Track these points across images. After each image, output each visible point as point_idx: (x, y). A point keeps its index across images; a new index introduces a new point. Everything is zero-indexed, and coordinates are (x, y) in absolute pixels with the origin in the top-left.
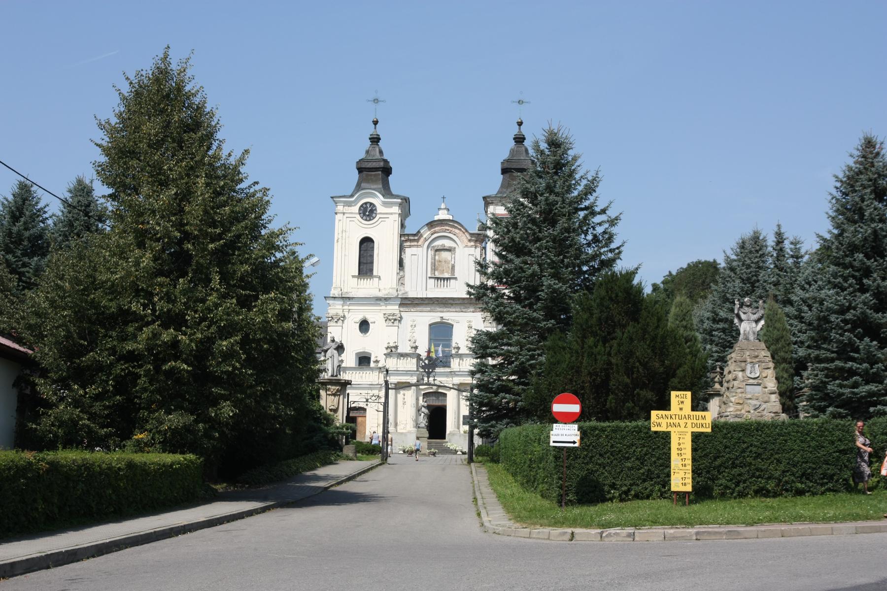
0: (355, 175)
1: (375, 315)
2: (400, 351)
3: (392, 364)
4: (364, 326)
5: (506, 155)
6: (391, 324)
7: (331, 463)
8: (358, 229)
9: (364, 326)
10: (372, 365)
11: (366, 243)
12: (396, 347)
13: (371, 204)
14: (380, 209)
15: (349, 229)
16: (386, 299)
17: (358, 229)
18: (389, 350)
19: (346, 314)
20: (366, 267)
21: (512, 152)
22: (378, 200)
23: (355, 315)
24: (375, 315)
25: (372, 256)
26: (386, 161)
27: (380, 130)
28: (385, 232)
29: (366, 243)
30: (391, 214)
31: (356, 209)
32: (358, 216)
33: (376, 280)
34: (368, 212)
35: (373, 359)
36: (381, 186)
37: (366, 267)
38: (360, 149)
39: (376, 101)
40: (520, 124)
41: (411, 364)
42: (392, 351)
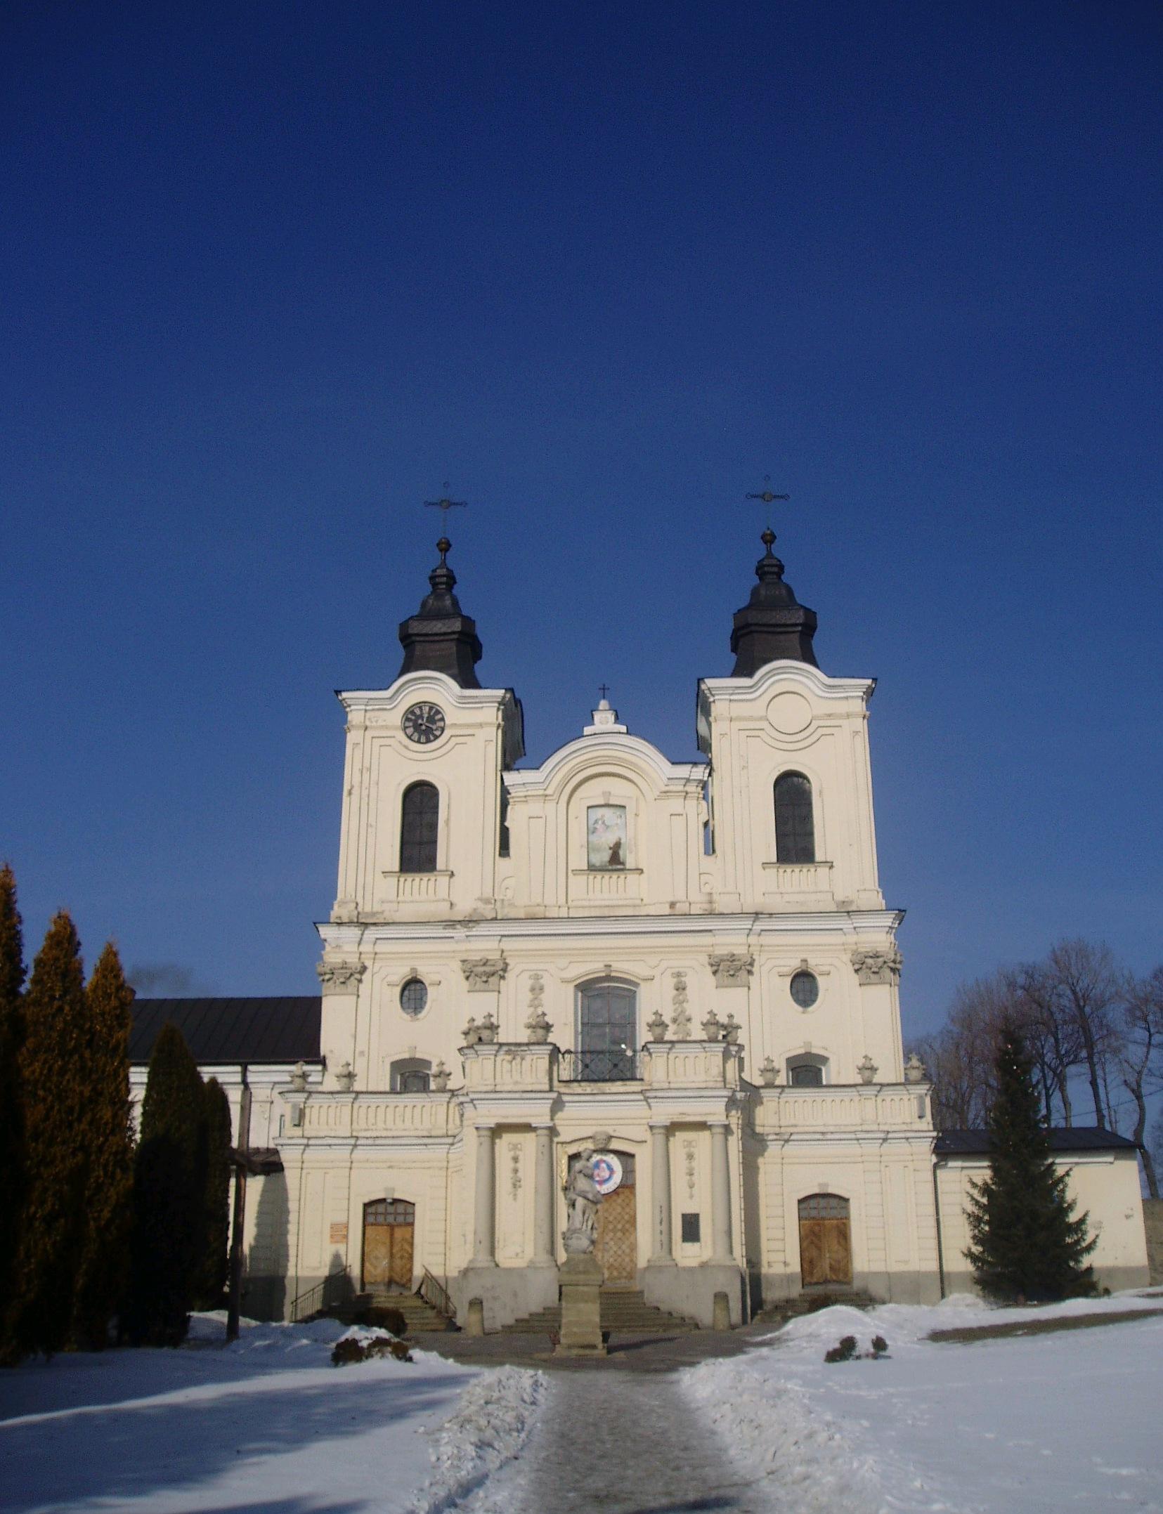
2: (502, 1037)
3: (481, 1072)
4: (413, 992)
6: (480, 985)
7: (80, 971)
9: (413, 992)
10: (433, 1086)
11: (420, 803)
12: (493, 1028)
13: (432, 706)
17: (404, 764)
18: (473, 1038)
19: (368, 963)
20: (418, 851)
25: (433, 827)
26: (468, 622)
28: (465, 761)
29: (420, 803)
30: (481, 725)
31: (396, 717)
32: (401, 735)
33: (443, 880)
34: (424, 724)
35: (434, 1069)
36: (455, 671)
37: (418, 851)
40: (769, 539)
41: (534, 1068)
42: (481, 1036)
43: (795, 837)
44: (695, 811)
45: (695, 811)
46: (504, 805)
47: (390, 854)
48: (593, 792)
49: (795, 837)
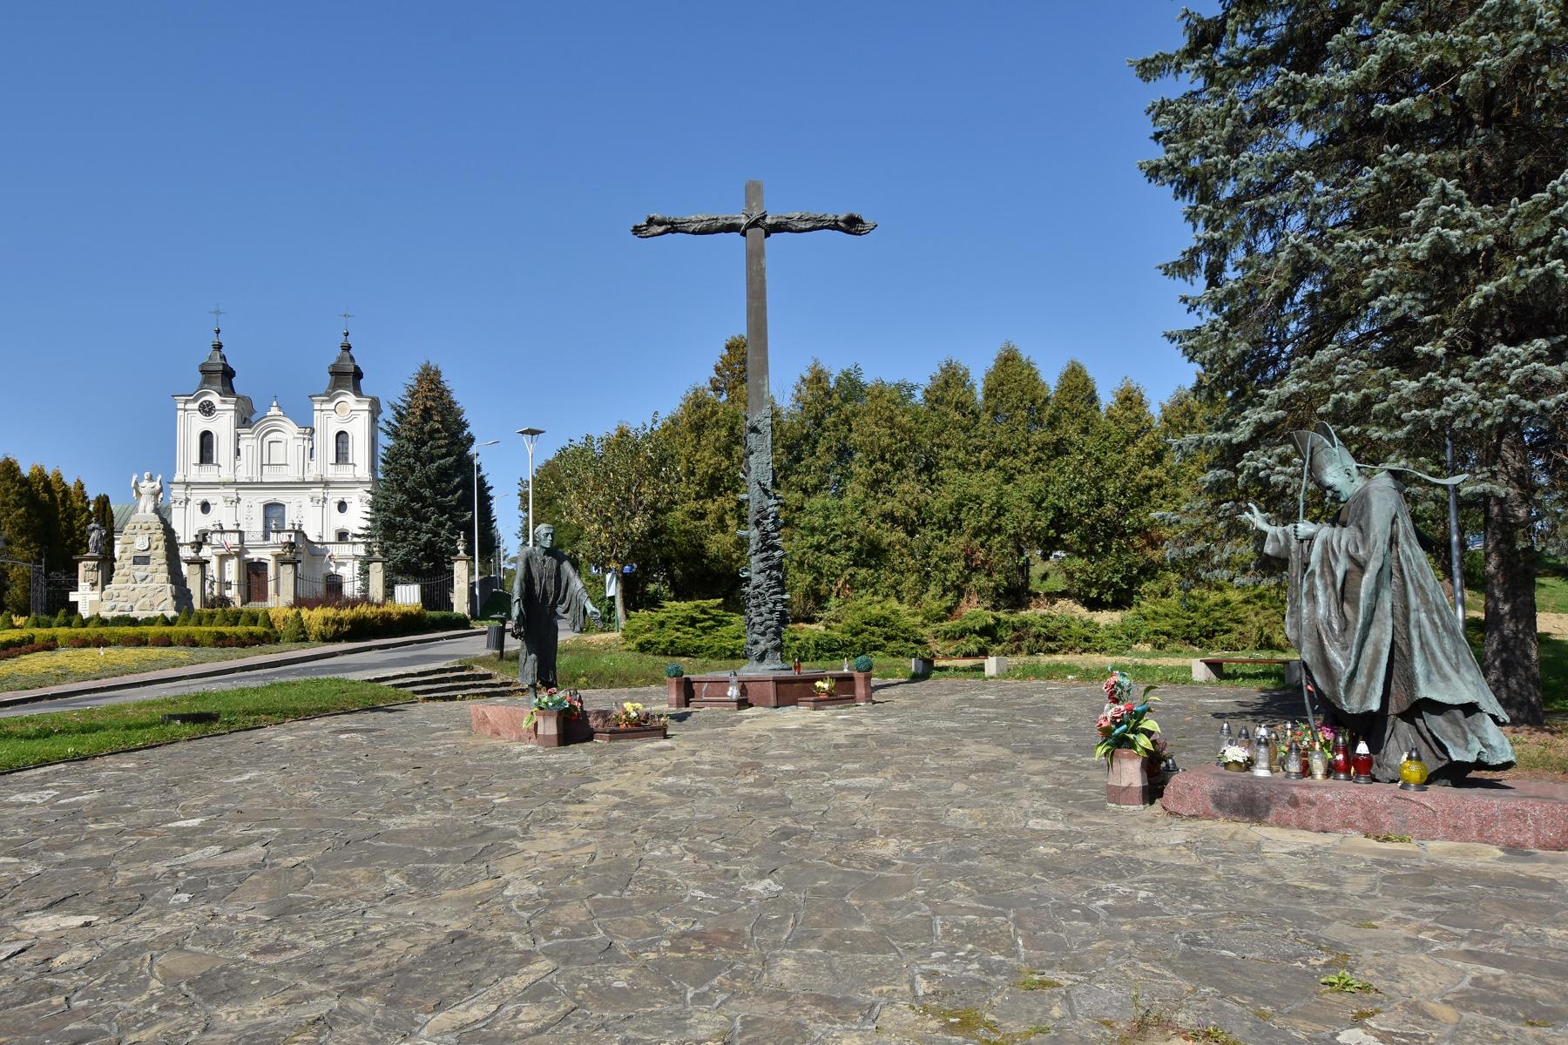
0: (200, 376)
1: (212, 496)
5: (333, 361)
8: (199, 423)
9: (205, 507)
11: (206, 437)
14: (218, 406)
15: (191, 424)
16: (224, 484)
17: (199, 423)
20: (206, 455)
21: (340, 359)
22: (214, 398)
23: (198, 496)
24: (212, 496)
27: (222, 339)
28: (223, 424)
29: (206, 437)
31: (196, 406)
34: (207, 409)
36: (220, 388)
37: (206, 455)
38: (333, 355)
39: (217, 312)
43: (341, 456)
44: (308, 445)
45: (308, 445)
46: (237, 441)
47: (196, 457)
48: (272, 436)
49: (341, 456)
